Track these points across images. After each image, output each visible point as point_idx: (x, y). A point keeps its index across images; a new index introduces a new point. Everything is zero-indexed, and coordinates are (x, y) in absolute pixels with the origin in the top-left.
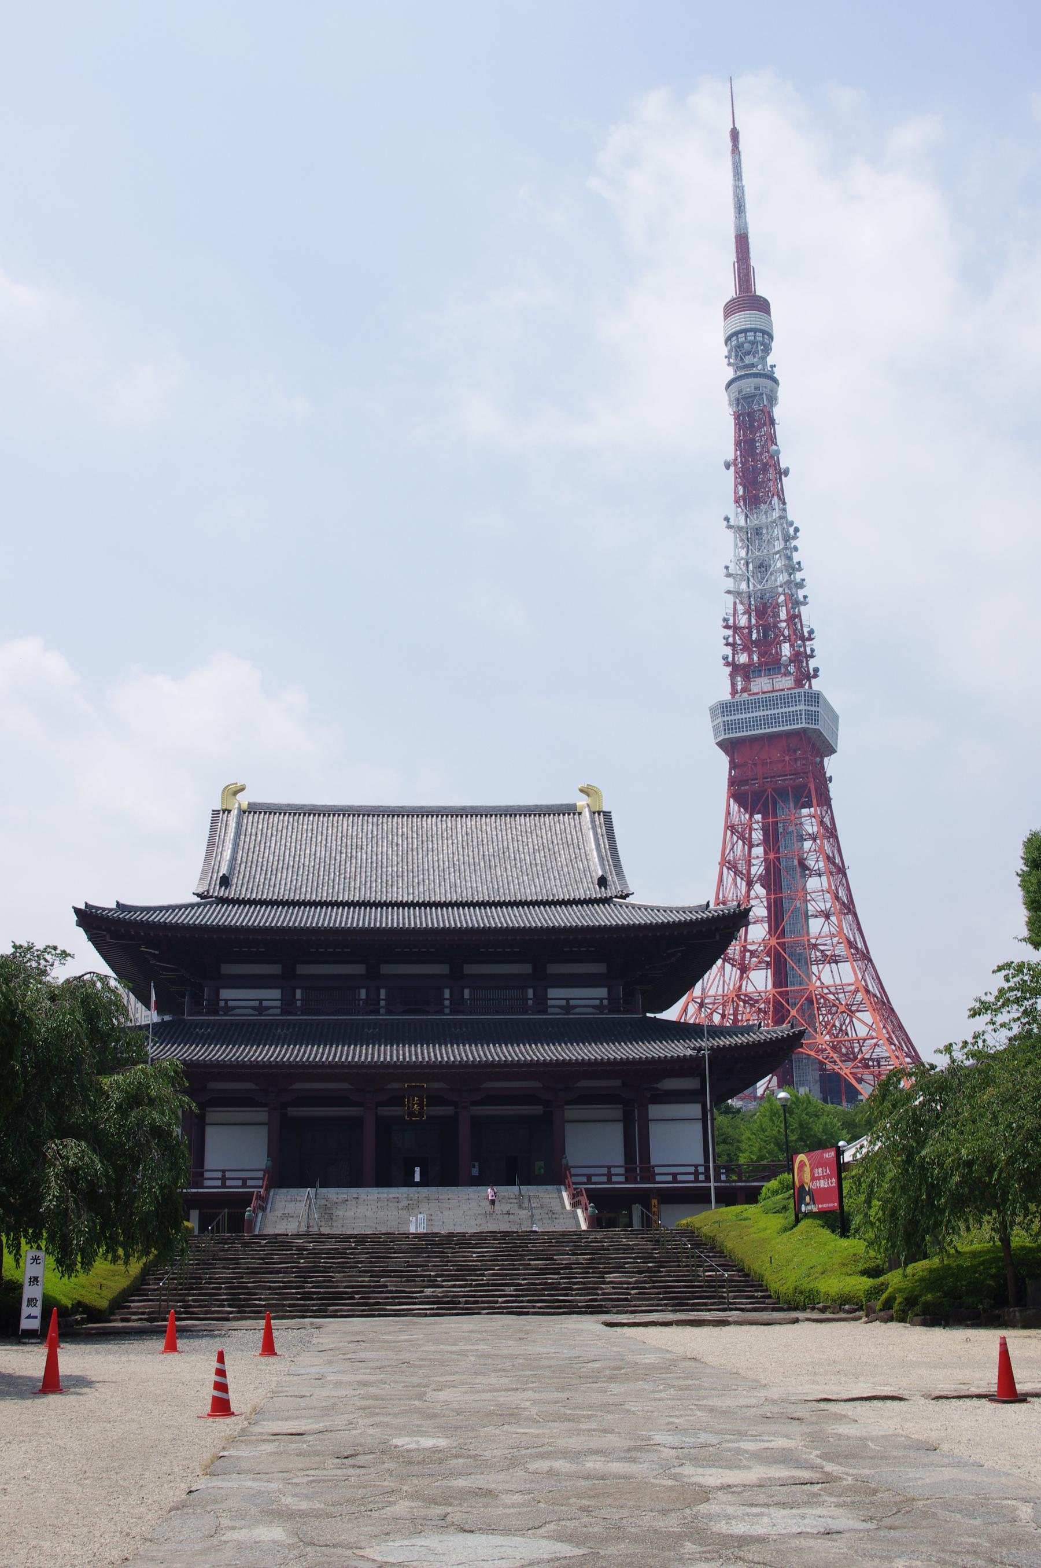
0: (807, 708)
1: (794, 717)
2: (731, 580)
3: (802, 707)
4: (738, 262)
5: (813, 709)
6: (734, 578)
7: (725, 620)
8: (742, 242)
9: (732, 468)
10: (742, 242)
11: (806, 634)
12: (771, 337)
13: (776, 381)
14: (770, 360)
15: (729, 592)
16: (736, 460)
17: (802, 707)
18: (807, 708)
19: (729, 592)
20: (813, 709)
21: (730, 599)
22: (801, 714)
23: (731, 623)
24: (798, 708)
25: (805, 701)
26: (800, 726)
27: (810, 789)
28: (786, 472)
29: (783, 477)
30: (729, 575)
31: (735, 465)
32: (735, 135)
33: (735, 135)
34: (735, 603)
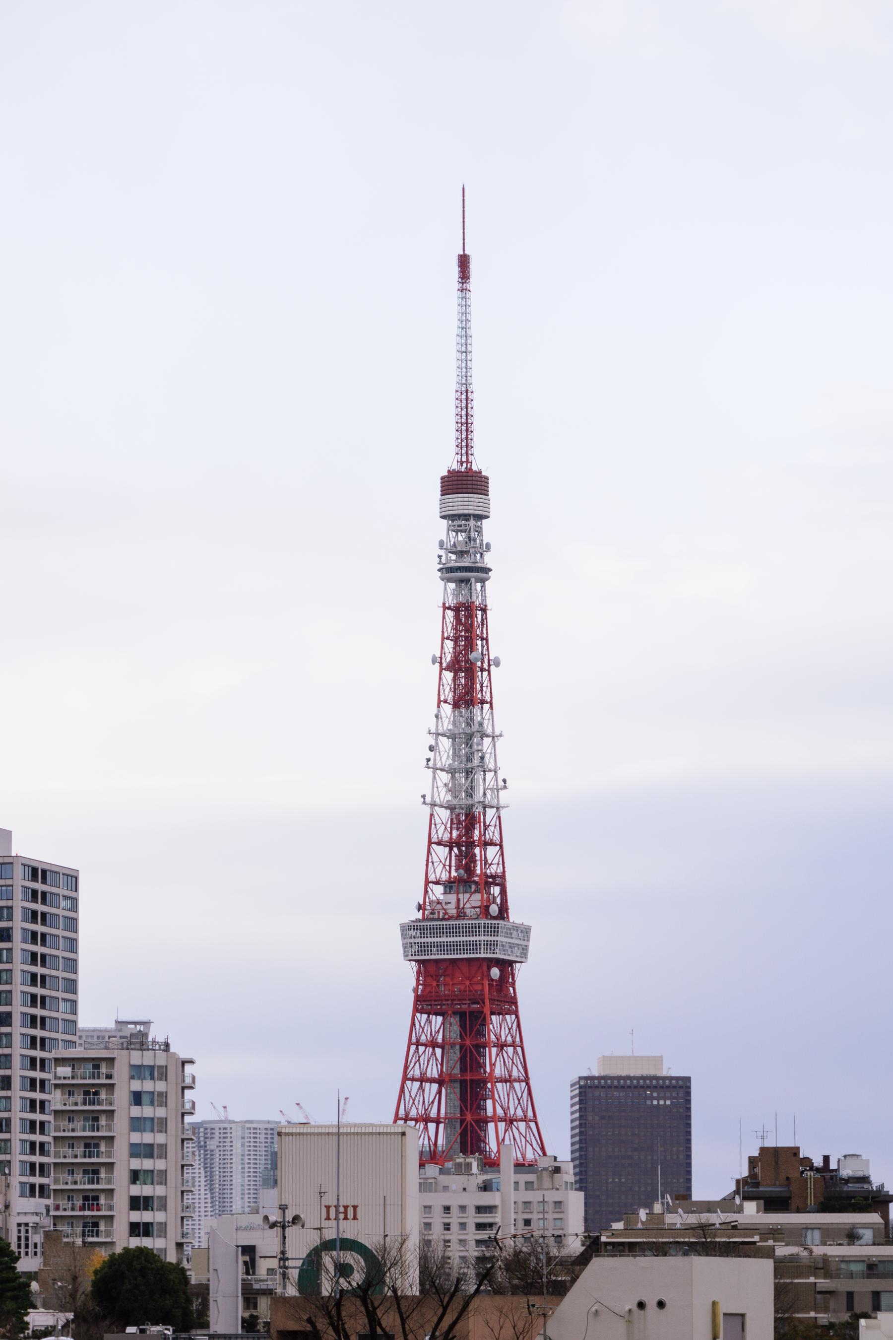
0: (486, 938)
1: (475, 946)
3: (482, 938)
5: (492, 938)
8: (465, 398)
9: (437, 665)
10: (465, 398)
17: (482, 938)
20: (492, 938)
22: (480, 945)
24: (477, 938)
25: (484, 931)
27: (484, 1019)
29: (493, 668)
32: (464, 262)
33: (464, 262)
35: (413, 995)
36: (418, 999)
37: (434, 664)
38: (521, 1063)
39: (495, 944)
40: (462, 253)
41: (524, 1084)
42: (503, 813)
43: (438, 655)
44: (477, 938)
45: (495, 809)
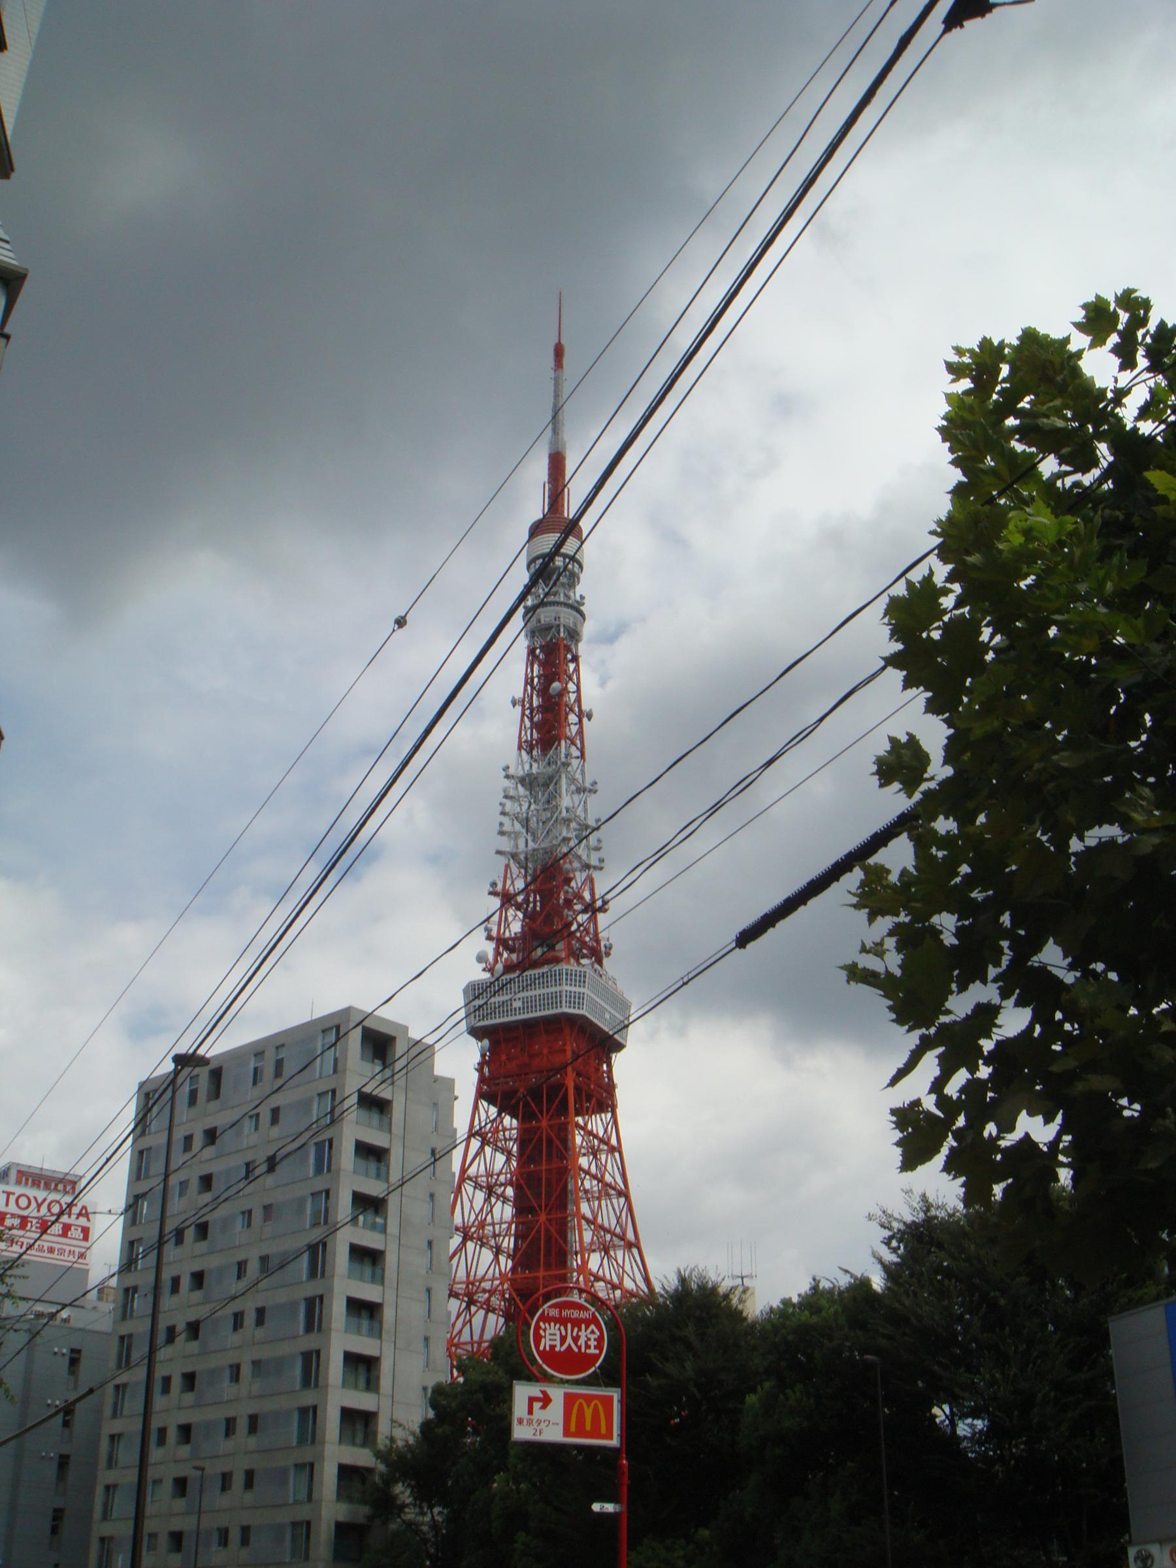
0: (568, 988)
1: (555, 999)
2: (505, 838)
4: (549, 483)
5: (577, 989)
6: (509, 836)
7: (494, 884)
9: (519, 708)
11: (599, 903)
12: (581, 567)
13: (582, 615)
14: (580, 590)
15: (499, 852)
16: (523, 700)
18: (568, 988)
19: (499, 852)
20: (577, 989)
21: (503, 861)
23: (499, 888)
24: (558, 989)
26: (559, 1011)
27: (567, 1090)
28: (589, 717)
29: (585, 720)
30: (502, 833)
31: (523, 706)
32: (559, 352)
33: (559, 352)
34: (507, 866)
35: (476, 1075)
36: (482, 1080)
37: (514, 706)
38: (618, 1169)
39: (581, 996)
40: (557, 341)
41: (622, 1200)
42: (596, 875)
43: (519, 694)
44: (558, 989)
45: (584, 875)
